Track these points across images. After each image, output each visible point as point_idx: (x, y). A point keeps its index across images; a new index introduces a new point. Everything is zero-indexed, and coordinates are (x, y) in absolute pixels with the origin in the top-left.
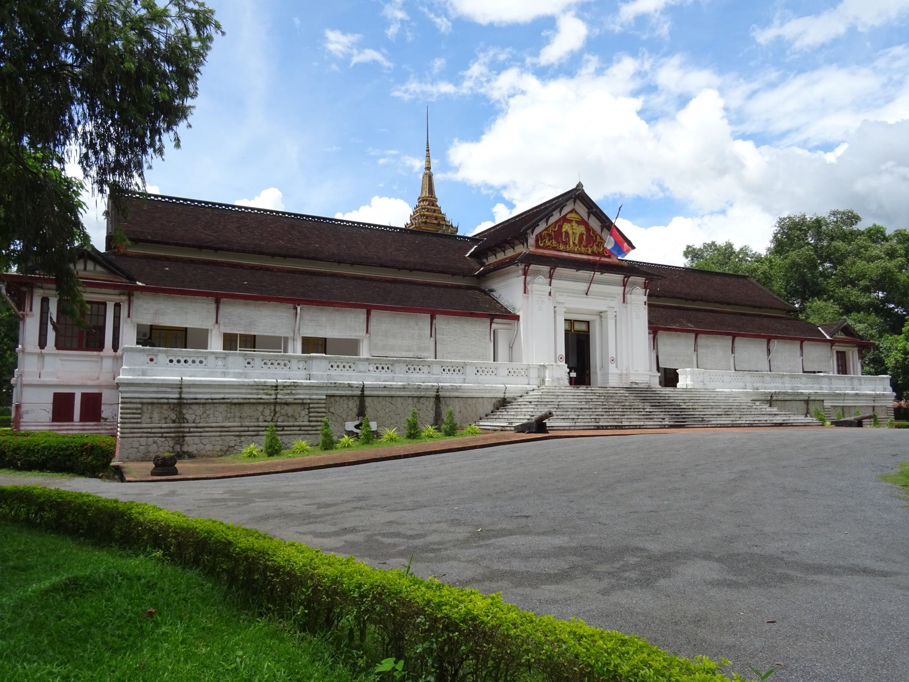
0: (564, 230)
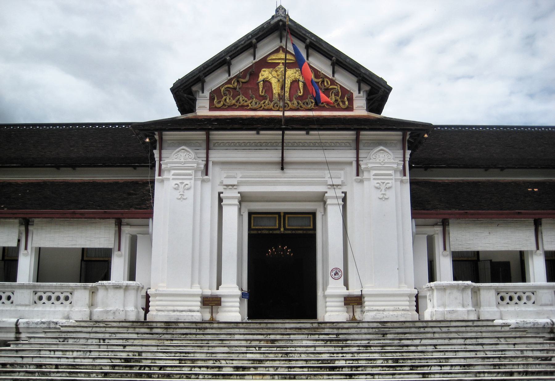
0: (261, 78)
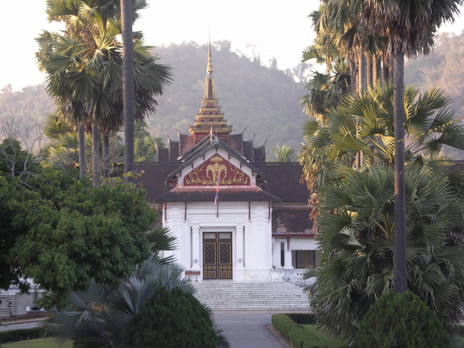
0: (207, 170)
